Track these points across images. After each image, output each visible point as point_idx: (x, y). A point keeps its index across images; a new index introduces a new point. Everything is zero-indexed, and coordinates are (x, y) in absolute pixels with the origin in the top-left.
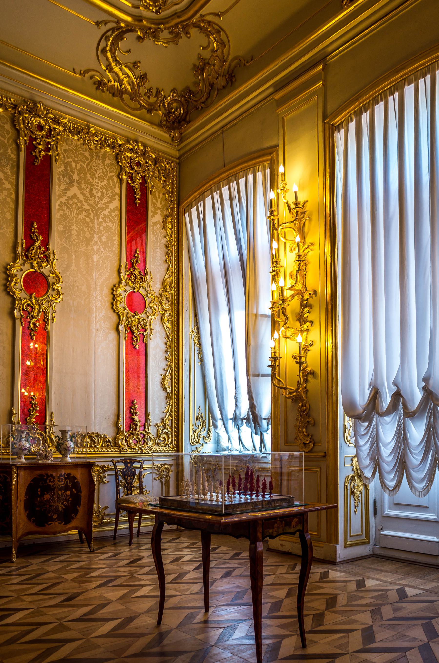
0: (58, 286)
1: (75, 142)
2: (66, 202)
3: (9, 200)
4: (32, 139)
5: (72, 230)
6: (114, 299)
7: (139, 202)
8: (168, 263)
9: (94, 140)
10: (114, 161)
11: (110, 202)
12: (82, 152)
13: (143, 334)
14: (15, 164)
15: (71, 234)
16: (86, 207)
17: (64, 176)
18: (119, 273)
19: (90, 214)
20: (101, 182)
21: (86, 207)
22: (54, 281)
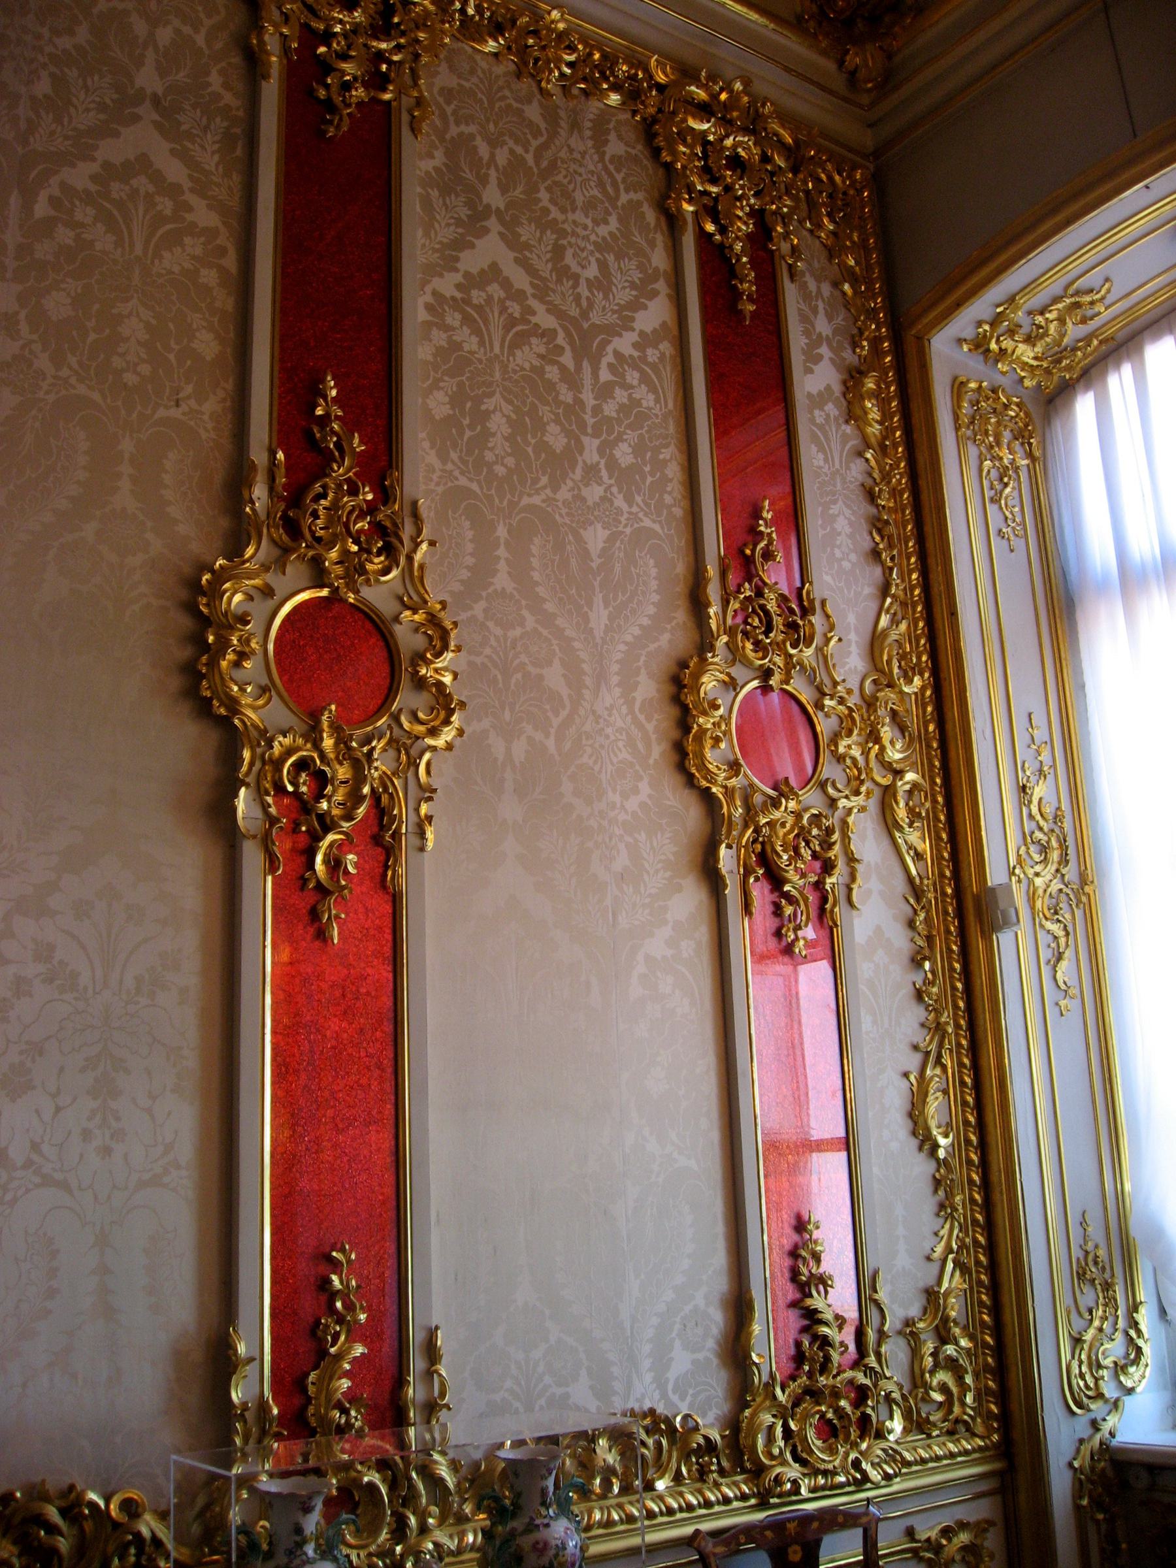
0: (443, 669)
1: (484, 65)
2: (458, 295)
3: (209, 277)
4: (312, 37)
5: (488, 414)
6: (684, 722)
7: (751, 308)
8: (883, 564)
9: (560, 60)
10: (640, 147)
11: (636, 306)
12: (515, 105)
13: (818, 886)
14: (238, 131)
15: (487, 434)
16: (544, 319)
17: (446, 191)
18: (697, 604)
19: (560, 350)
20: (596, 223)
21: (544, 319)
22: (419, 641)
